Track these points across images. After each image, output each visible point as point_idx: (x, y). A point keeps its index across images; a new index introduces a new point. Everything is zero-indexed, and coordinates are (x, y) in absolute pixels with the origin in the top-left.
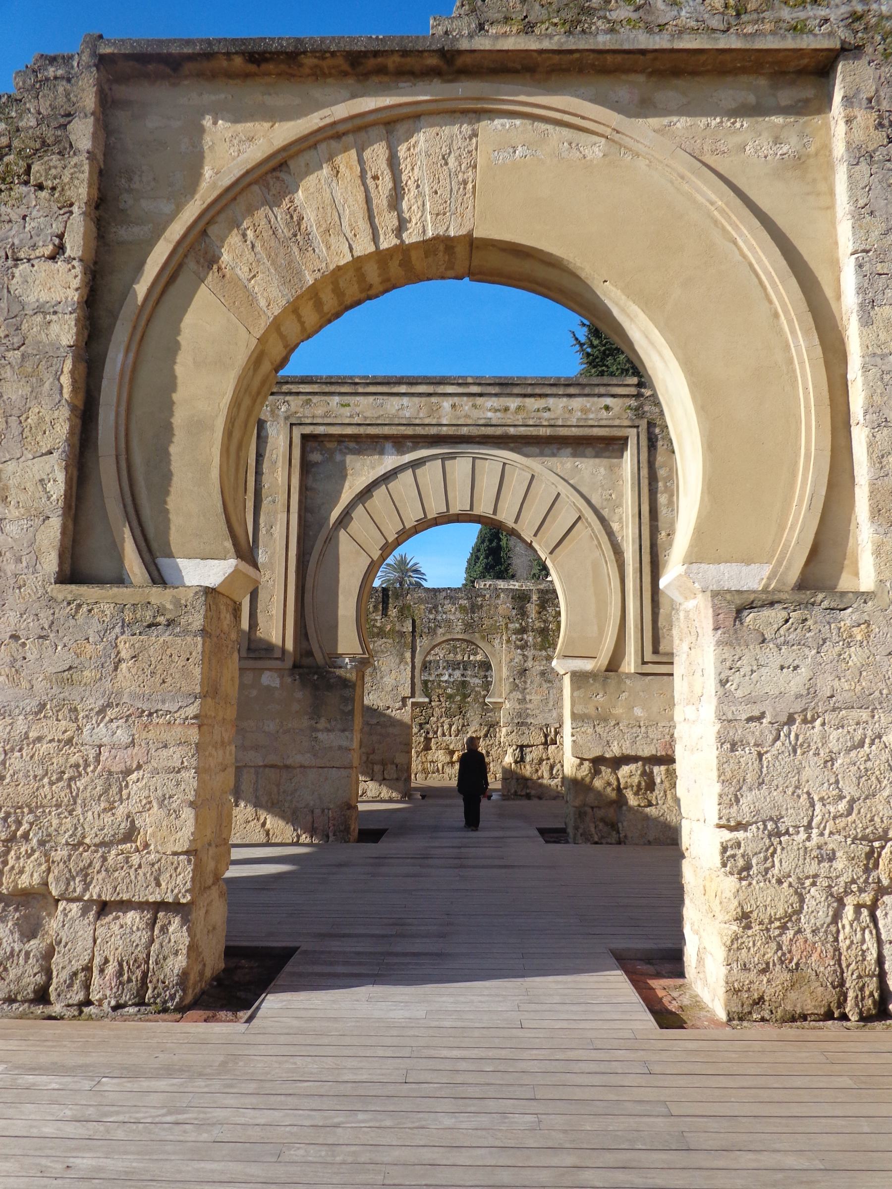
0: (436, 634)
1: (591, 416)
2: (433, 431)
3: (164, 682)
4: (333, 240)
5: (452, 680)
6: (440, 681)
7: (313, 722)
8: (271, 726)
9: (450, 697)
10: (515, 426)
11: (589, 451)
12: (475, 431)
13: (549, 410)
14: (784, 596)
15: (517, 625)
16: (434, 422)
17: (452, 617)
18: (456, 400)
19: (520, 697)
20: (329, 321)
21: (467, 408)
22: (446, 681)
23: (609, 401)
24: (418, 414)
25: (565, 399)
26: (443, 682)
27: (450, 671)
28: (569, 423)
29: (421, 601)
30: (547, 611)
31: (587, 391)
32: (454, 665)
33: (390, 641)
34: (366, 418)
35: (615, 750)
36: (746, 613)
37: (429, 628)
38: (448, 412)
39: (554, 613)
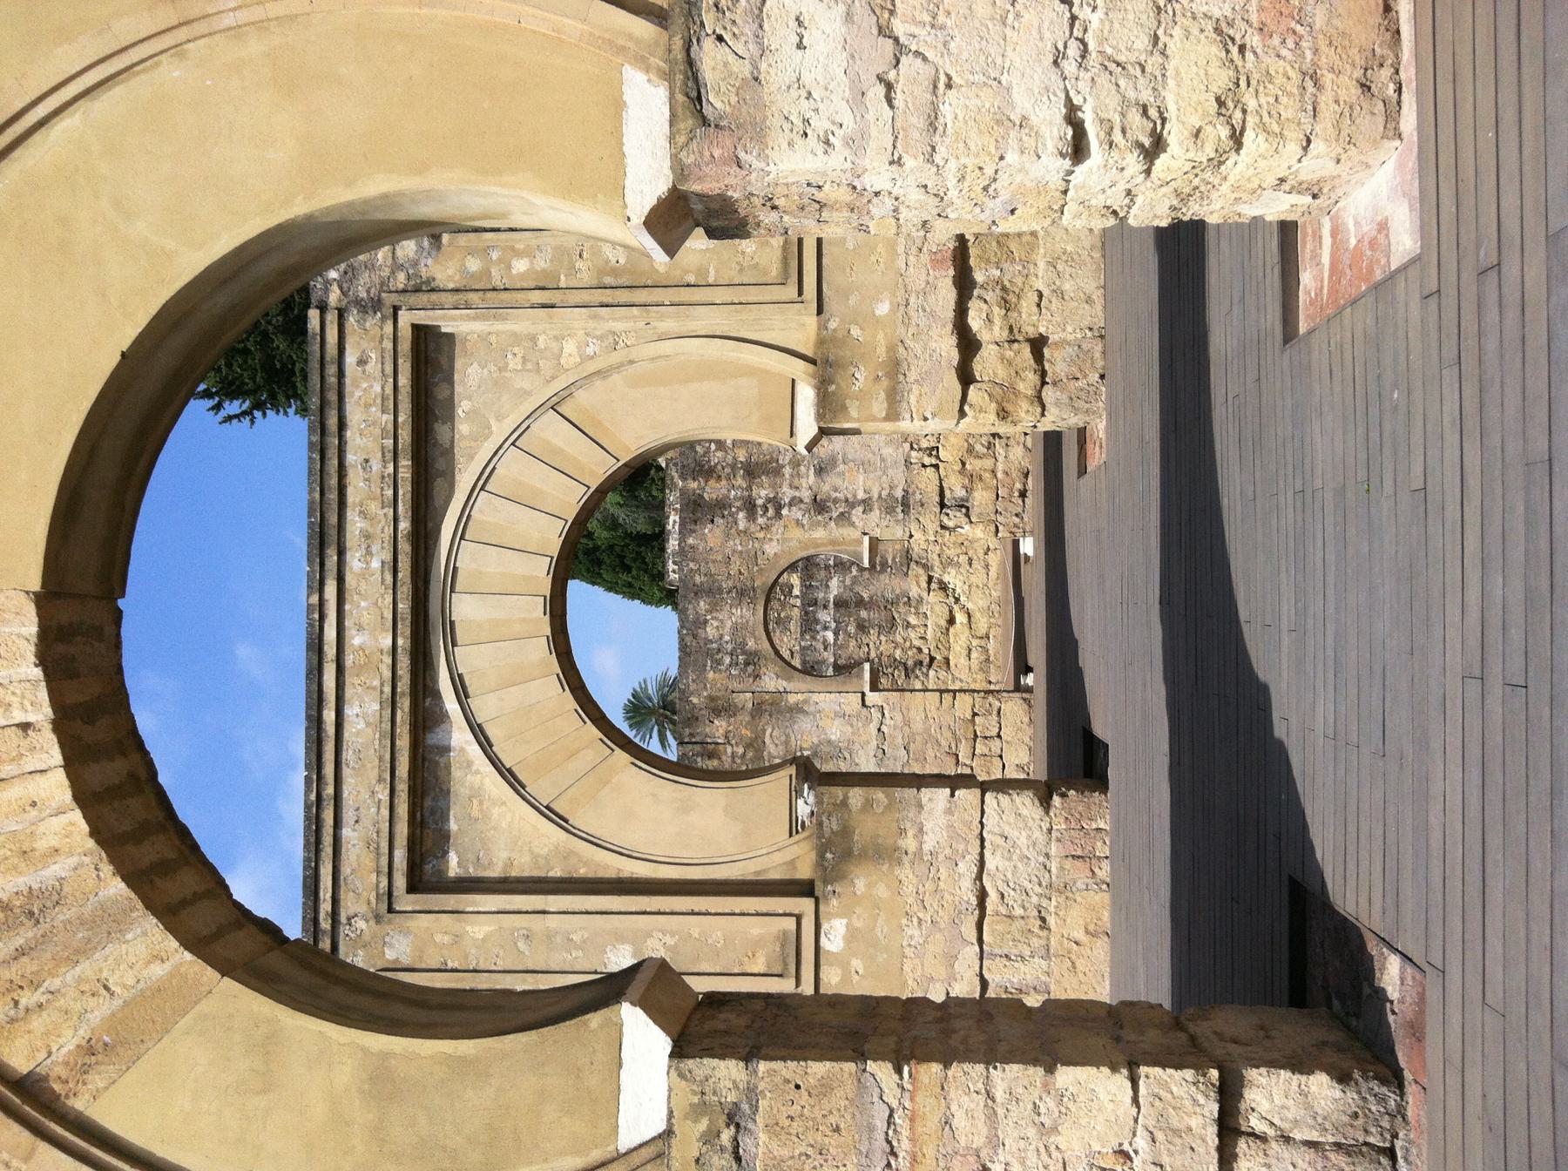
0: (756, 653)
1: (378, 389)
2: (404, 663)
3: (837, 1130)
4: (42, 845)
5: (833, 625)
7: (905, 858)
9: (862, 627)
10: (396, 520)
11: (441, 393)
12: (405, 590)
13: (367, 461)
14: (678, 43)
15: (741, 515)
17: (729, 624)
19: (861, 509)
20: (195, 847)
22: (836, 634)
23: (350, 359)
24: (374, 688)
28: (390, 427)
29: (701, 678)
31: (332, 396)
32: (809, 625)
34: (380, 780)
35: (947, 347)
36: (707, 110)
37: (747, 664)
38: (371, 632)
39: (719, 454)
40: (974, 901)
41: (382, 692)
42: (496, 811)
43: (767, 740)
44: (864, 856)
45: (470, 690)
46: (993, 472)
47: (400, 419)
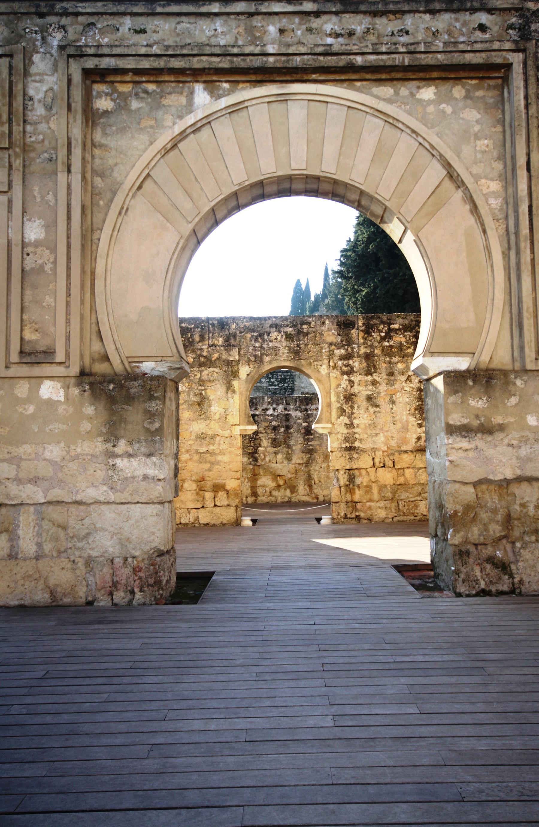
0: (261, 361)
1: (462, 39)
2: (257, 62)
5: (276, 414)
6: (266, 415)
7: (109, 445)
8: (54, 452)
9: (275, 428)
10: (363, 54)
13: (407, 33)
15: (343, 351)
16: (257, 50)
17: (278, 345)
18: (284, 22)
19: (348, 422)
21: (299, 32)
22: (271, 415)
23: (483, 18)
25: (427, 17)
26: (268, 415)
27: (274, 406)
28: (434, 49)
30: (371, 336)
33: (216, 370)
34: (167, 47)
37: (255, 356)
39: (379, 338)
40: (79, 498)
41: (233, 46)
42: (145, 138)
43: (211, 369)
44: (112, 412)
45: (234, 115)
46: (371, 500)
47: (439, 56)
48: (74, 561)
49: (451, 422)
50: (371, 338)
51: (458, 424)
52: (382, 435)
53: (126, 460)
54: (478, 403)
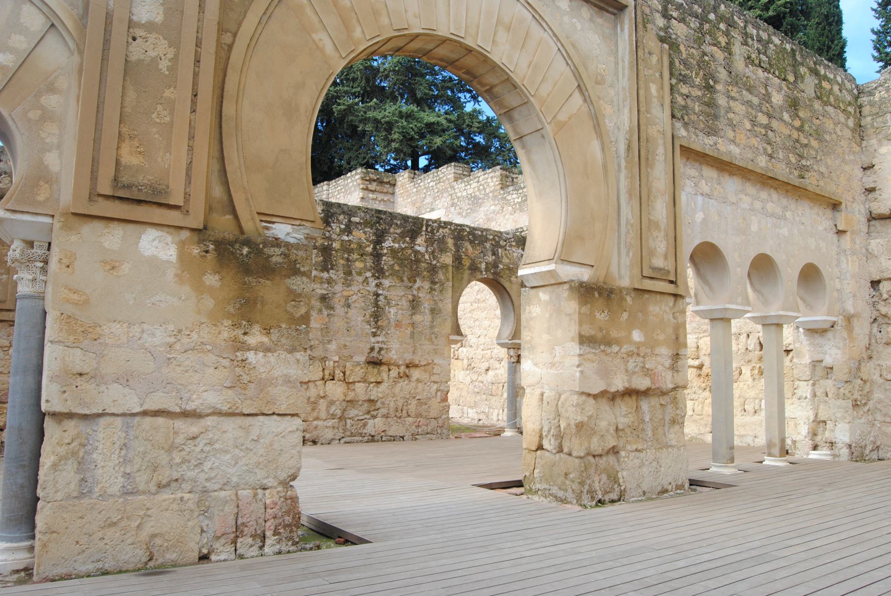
7: (240, 332)
39: (338, 230)
40: (190, 407)
46: (317, 419)
48: (182, 499)
49: (583, 333)
50: (329, 229)
51: (588, 335)
52: (334, 342)
53: (261, 354)
54: (602, 317)
